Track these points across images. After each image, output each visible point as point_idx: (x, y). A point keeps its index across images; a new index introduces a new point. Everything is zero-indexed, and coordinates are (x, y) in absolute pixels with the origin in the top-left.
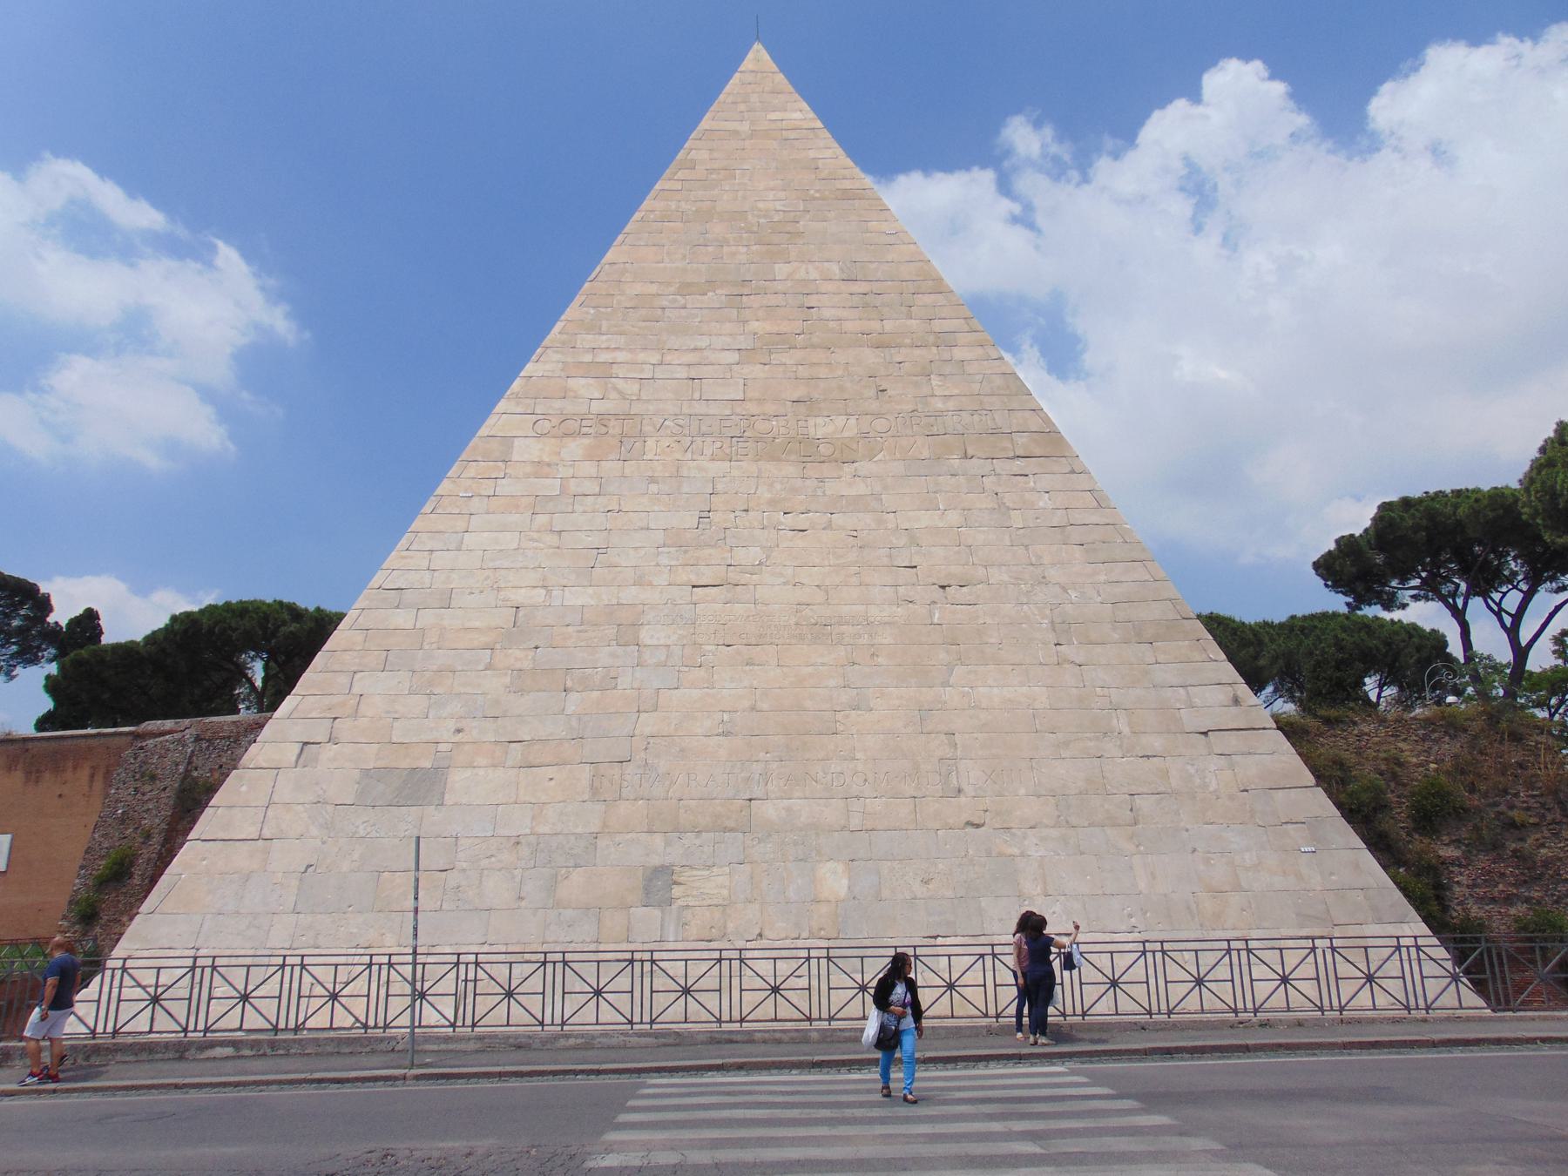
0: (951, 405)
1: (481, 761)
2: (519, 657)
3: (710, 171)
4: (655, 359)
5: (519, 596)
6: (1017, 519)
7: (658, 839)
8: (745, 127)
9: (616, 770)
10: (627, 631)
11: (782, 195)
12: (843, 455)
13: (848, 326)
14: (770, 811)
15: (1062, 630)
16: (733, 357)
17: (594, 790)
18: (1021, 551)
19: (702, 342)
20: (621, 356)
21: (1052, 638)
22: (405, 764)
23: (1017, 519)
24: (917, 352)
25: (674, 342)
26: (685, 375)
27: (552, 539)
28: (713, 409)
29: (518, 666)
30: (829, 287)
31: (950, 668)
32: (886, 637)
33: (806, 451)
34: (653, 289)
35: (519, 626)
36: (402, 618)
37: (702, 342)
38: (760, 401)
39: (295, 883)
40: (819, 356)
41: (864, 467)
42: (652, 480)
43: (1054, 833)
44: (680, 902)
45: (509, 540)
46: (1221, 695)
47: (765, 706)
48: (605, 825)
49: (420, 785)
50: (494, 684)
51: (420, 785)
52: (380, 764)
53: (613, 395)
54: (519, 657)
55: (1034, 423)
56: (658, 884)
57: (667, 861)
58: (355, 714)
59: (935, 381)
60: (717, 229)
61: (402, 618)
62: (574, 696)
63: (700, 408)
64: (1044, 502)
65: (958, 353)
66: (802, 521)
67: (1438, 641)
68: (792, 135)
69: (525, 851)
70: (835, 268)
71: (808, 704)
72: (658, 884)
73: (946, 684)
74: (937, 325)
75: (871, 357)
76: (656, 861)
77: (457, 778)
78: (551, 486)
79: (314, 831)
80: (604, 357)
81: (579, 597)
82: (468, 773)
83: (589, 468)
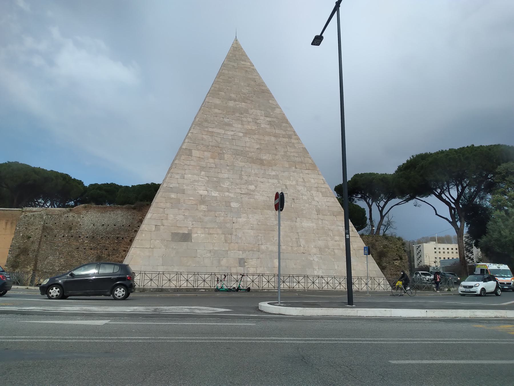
0: (292, 154)
1: (199, 232)
2: (203, 207)
3: (229, 78)
4: (223, 132)
6: (307, 184)
7: (241, 252)
8: (235, 65)
9: (230, 236)
10: (228, 204)
11: (248, 88)
12: (270, 164)
13: (267, 130)
14: (263, 247)
15: (318, 211)
16: (241, 135)
17: (226, 241)
18: (309, 192)
19: (234, 129)
20: (215, 130)
21: (316, 213)
22: (181, 232)
23: (307, 184)
24: (284, 139)
26: (231, 138)
27: (207, 178)
28: (239, 148)
29: (204, 210)
31: (296, 218)
33: (261, 162)
34: (220, 112)
35: (202, 200)
36: (173, 196)
38: (249, 147)
39: (161, 259)
41: (274, 168)
42: (228, 166)
43: (319, 256)
44: (247, 266)
45: (196, 177)
47: (260, 224)
48: (229, 248)
49: (186, 237)
51: (186, 237)
52: (175, 231)
53: (214, 141)
55: (310, 161)
56: (242, 262)
57: (243, 257)
58: (167, 219)
59: (288, 148)
61: (173, 196)
62: (218, 218)
63: (235, 147)
64: (312, 181)
66: (262, 180)
67: (363, 211)
68: (248, 70)
69: (212, 254)
70: (263, 112)
71: (268, 224)
72: (242, 262)
73: (296, 222)
75: (273, 139)
76: (241, 257)
77: (194, 236)
78: (203, 164)
79: (163, 247)
80: (210, 130)
81: (215, 194)
82: (196, 235)
83: (211, 160)
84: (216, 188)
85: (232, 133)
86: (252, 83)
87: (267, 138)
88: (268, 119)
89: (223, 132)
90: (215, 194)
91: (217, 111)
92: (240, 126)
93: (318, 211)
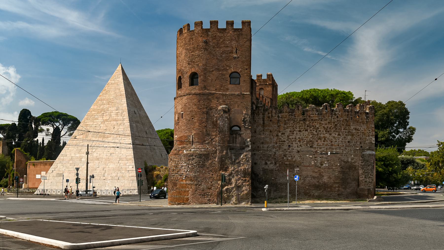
5: (73, 155)
8: (113, 82)
25: (95, 121)
30: (114, 111)
32: (104, 160)
36: (62, 158)
37: (98, 121)
40: (110, 122)
45: (73, 149)
46: (132, 167)
50: (69, 165)
54: (71, 162)
60: (104, 102)
65: (125, 122)
74: (124, 117)
75: (115, 122)
80: (87, 123)
81: (78, 155)
84: (79, 153)
85: (96, 123)
86: (118, 91)
87: (112, 122)
88: (117, 111)
89: (92, 123)
90: (78, 155)
91: (94, 112)
92: (102, 118)
93: (121, 159)
